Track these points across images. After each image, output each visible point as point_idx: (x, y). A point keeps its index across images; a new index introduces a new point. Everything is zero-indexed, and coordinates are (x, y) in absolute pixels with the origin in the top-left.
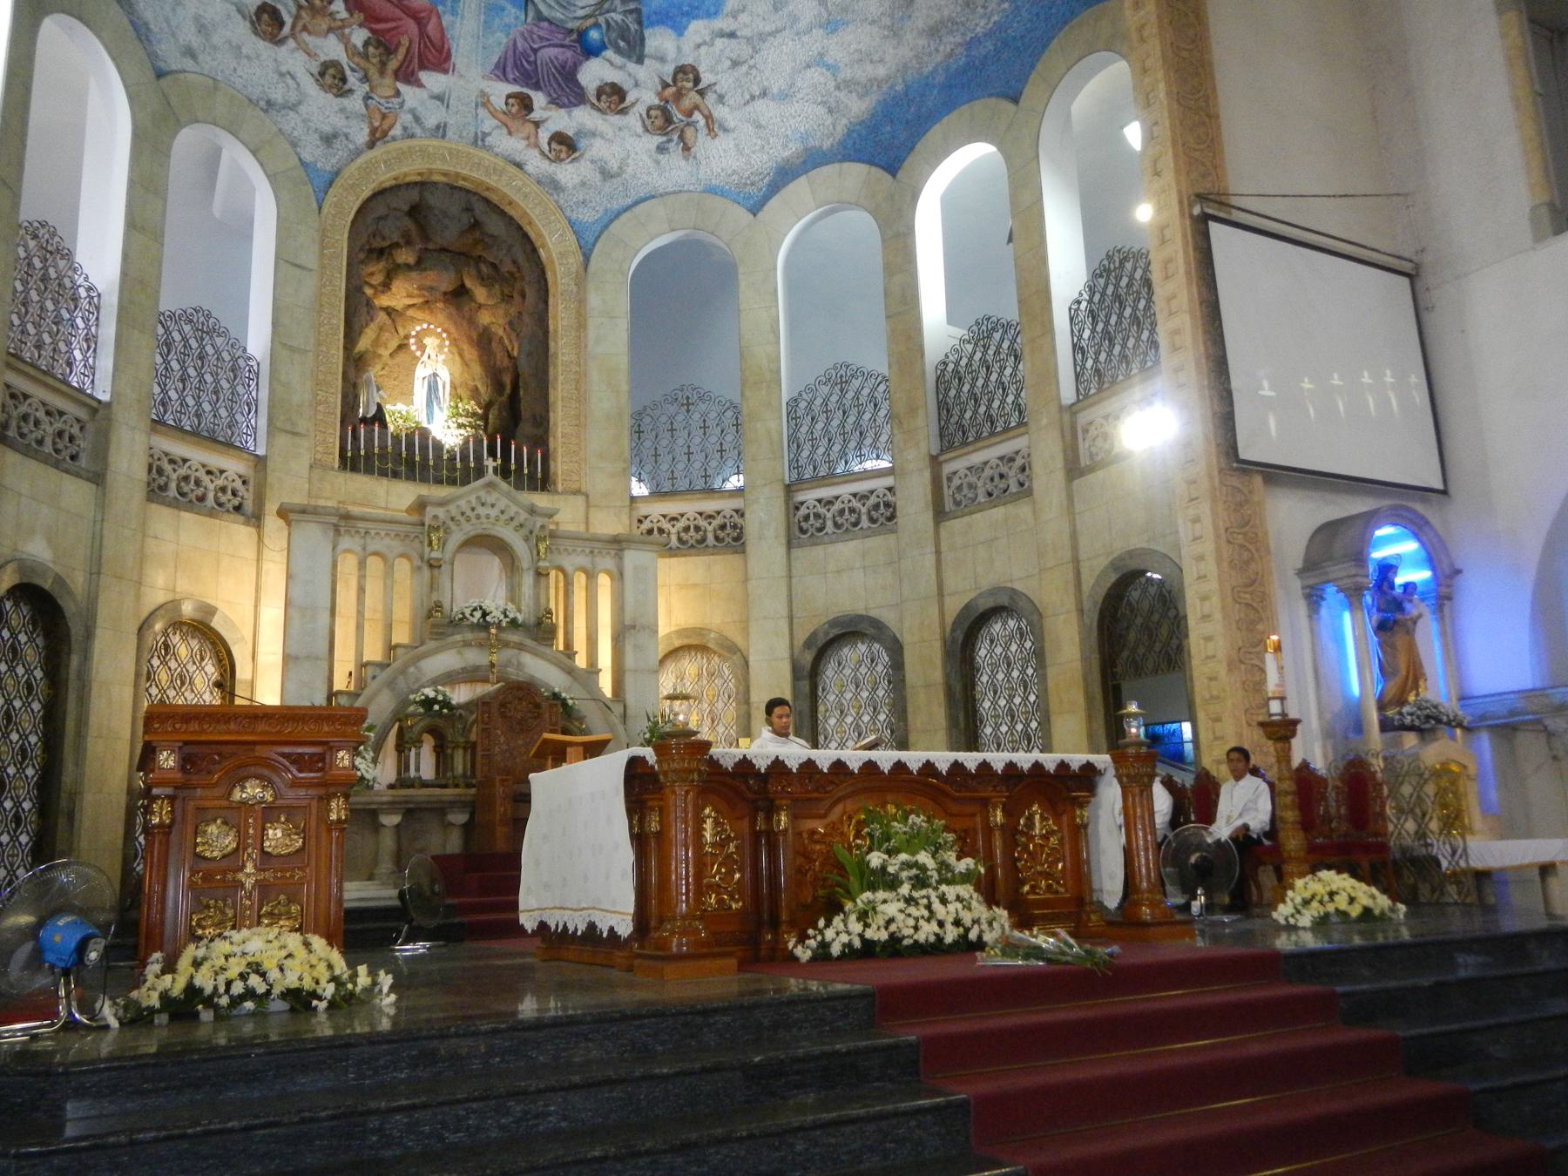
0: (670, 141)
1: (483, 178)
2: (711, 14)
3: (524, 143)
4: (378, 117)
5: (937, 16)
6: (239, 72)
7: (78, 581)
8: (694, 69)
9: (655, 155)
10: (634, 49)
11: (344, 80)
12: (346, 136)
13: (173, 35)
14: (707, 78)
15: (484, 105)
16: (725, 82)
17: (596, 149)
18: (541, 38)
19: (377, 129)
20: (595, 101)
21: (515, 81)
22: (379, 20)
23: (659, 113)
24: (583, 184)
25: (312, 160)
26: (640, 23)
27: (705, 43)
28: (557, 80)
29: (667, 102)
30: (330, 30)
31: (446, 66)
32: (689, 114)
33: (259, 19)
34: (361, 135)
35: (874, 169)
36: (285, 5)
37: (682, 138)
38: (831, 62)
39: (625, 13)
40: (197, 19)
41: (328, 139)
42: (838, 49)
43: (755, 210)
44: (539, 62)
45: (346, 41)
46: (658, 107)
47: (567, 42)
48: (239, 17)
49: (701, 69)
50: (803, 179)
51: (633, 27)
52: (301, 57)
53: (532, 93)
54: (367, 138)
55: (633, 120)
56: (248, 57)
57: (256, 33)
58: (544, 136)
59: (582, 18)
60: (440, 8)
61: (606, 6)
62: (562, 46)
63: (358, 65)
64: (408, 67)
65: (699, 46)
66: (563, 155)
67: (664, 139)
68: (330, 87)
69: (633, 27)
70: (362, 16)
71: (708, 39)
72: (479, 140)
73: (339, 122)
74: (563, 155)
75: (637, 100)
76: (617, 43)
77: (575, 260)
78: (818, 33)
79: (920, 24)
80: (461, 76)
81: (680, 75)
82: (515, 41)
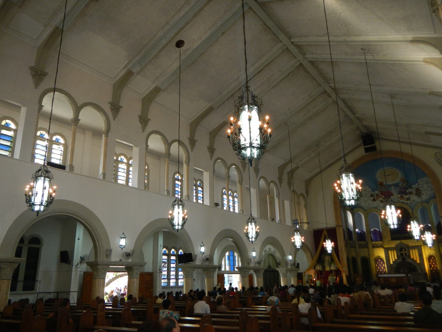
7: (368, 257)
10: (411, 188)
17: (411, 199)
45: (382, 198)
55: (414, 195)
57: (373, 201)
72: (399, 202)
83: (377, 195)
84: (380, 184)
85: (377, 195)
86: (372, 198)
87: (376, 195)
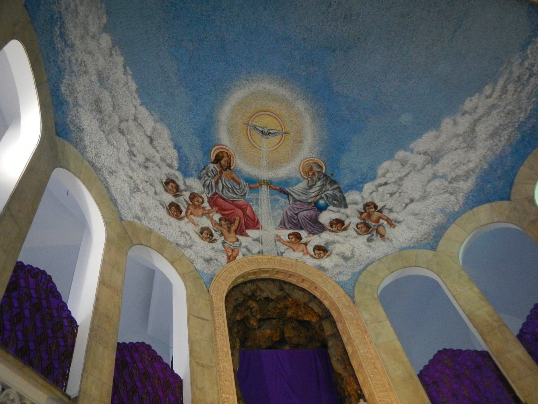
0: (373, 235)
1: (287, 269)
2: (373, 178)
3: (301, 254)
4: (230, 251)
5: (492, 128)
6: (162, 230)
8: (373, 203)
9: (367, 244)
10: (342, 203)
11: (212, 235)
12: (216, 259)
13: (129, 208)
14: (380, 205)
15: (278, 240)
16: (390, 203)
17: (337, 248)
18: (298, 209)
19: (230, 256)
20: (330, 228)
21: (291, 228)
22: (225, 210)
23: (362, 225)
24: (336, 265)
25: (202, 269)
26: (341, 192)
27: (373, 191)
28: (309, 224)
29: (364, 220)
30: (203, 214)
31: (258, 227)
32: (377, 221)
33: (170, 208)
34: (223, 259)
35: (493, 204)
36: (182, 203)
37: (378, 232)
38: (440, 174)
39: (333, 190)
40: (141, 204)
41: (208, 261)
42: (442, 167)
43: (433, 248)
44: (299, 219)
45: (211, 219)
46: (361, 223)
47: (310, 207)
48: (161, 207)
49: (377, 202)
50: (453, 225)
51: (338, 194)
52: (191, 225)
53: (300, 232)
54: (226, 261)
55: (351, 232)
56: (166, 225)
57: (169, 214)
58: (310, 249)
59: (314, 197)
60: (251, 203)
61: (324, 189)
62: (308, 210)
63: (217, 229)
64: (241, 229)
65: (371, 193)
66: (322, 255)
67: (369, 235)
68: (206, 238)
69: (338, 194)
70: (217, 208)
71: (374, 189)
73: (212, 254)
74: (322, 255)
75: (350, 223)
76: (333, 202)
77: (346, 300)
78: (429, 167)
79: (484, 136)
80: (266, 230)
81: (367, 208)
82: (287, 212)
83: (193, 196)
84: (217, 160)
85: (193, 196)
86: (169, 198)
87: (187, 195)
